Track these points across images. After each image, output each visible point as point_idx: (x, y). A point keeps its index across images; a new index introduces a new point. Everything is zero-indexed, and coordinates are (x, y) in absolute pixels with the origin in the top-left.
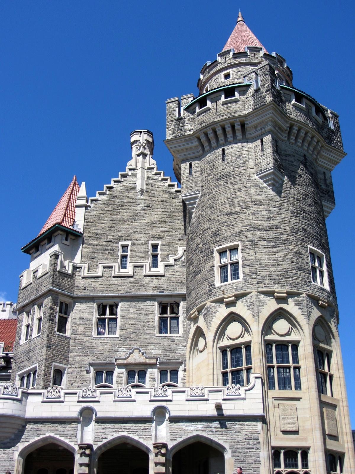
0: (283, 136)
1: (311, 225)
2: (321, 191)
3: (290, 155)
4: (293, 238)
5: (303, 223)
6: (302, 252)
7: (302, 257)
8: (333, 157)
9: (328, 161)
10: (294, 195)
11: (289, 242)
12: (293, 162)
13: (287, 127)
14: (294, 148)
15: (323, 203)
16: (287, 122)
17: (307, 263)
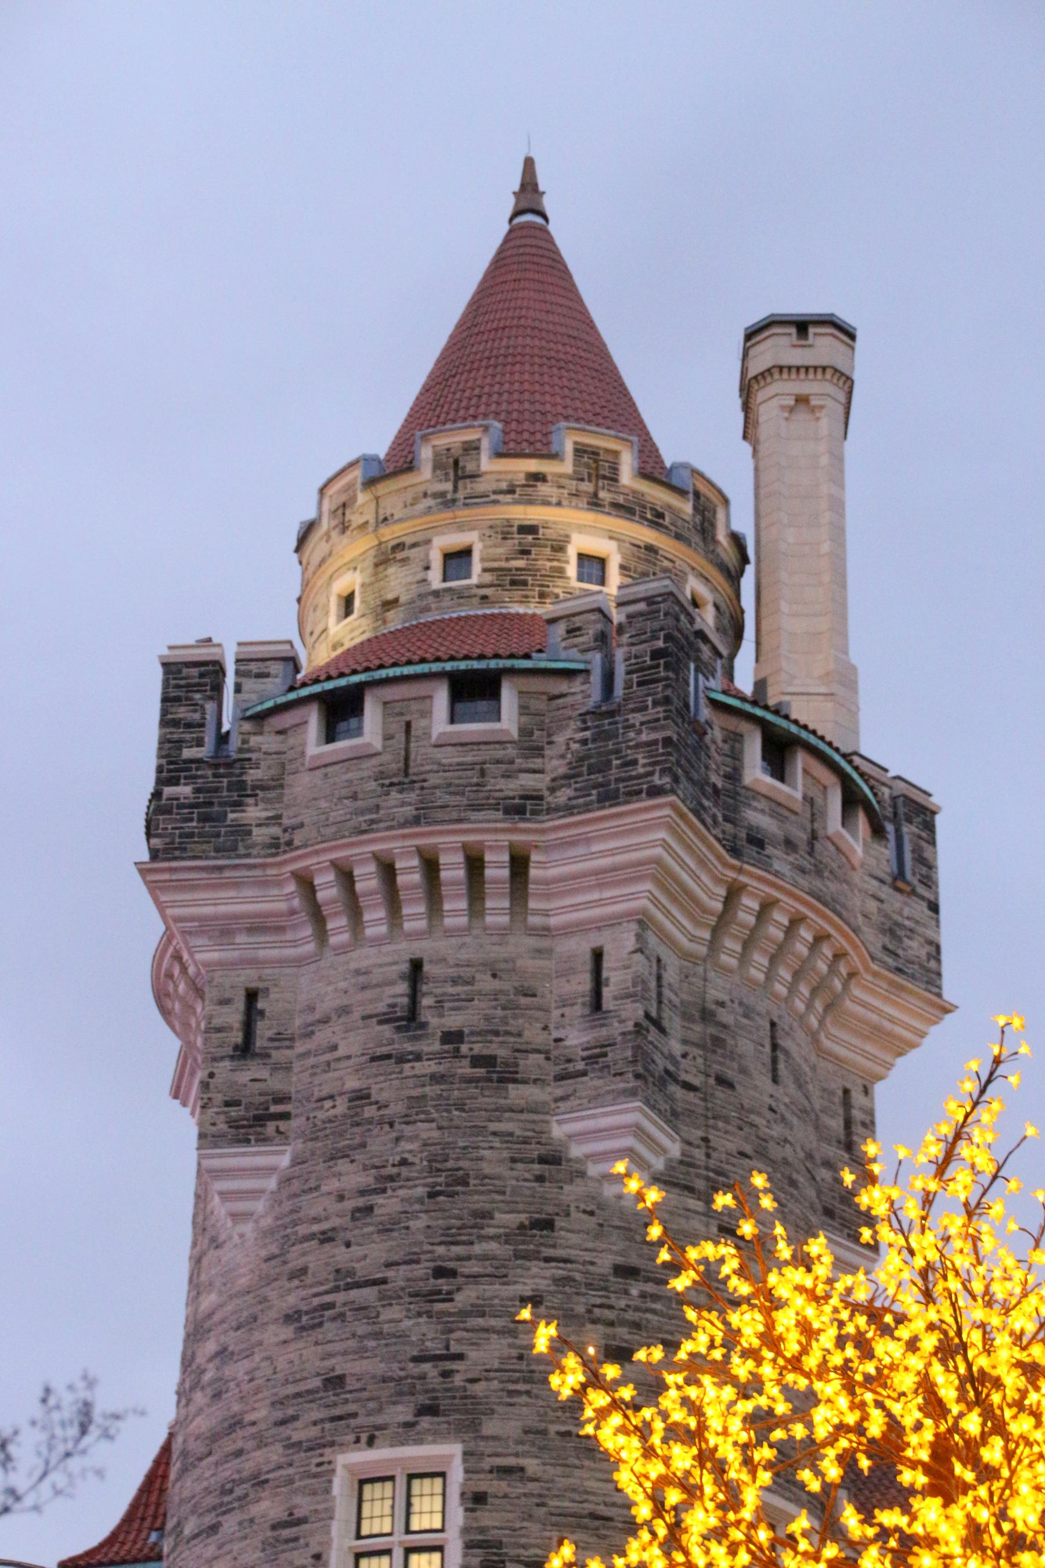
0: (295, 943)
1: (377, 1335)
2: (553, 1069)
3: (325, 1021)
4: (275, 1454)
5: (338, 1347)
6: (304, 1505)
7: (296, 1539)
8: (611, 852)
9: (601, 886)
10: (316, 1220)
11: (259, 1482)
12: (334, 1048)
13: (289, 897)
14: (353, 966)
15: (558, 1131)
16: (279, 884)
17: (317, 1557)
